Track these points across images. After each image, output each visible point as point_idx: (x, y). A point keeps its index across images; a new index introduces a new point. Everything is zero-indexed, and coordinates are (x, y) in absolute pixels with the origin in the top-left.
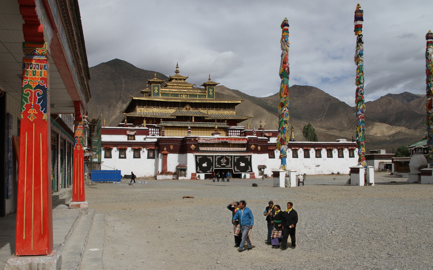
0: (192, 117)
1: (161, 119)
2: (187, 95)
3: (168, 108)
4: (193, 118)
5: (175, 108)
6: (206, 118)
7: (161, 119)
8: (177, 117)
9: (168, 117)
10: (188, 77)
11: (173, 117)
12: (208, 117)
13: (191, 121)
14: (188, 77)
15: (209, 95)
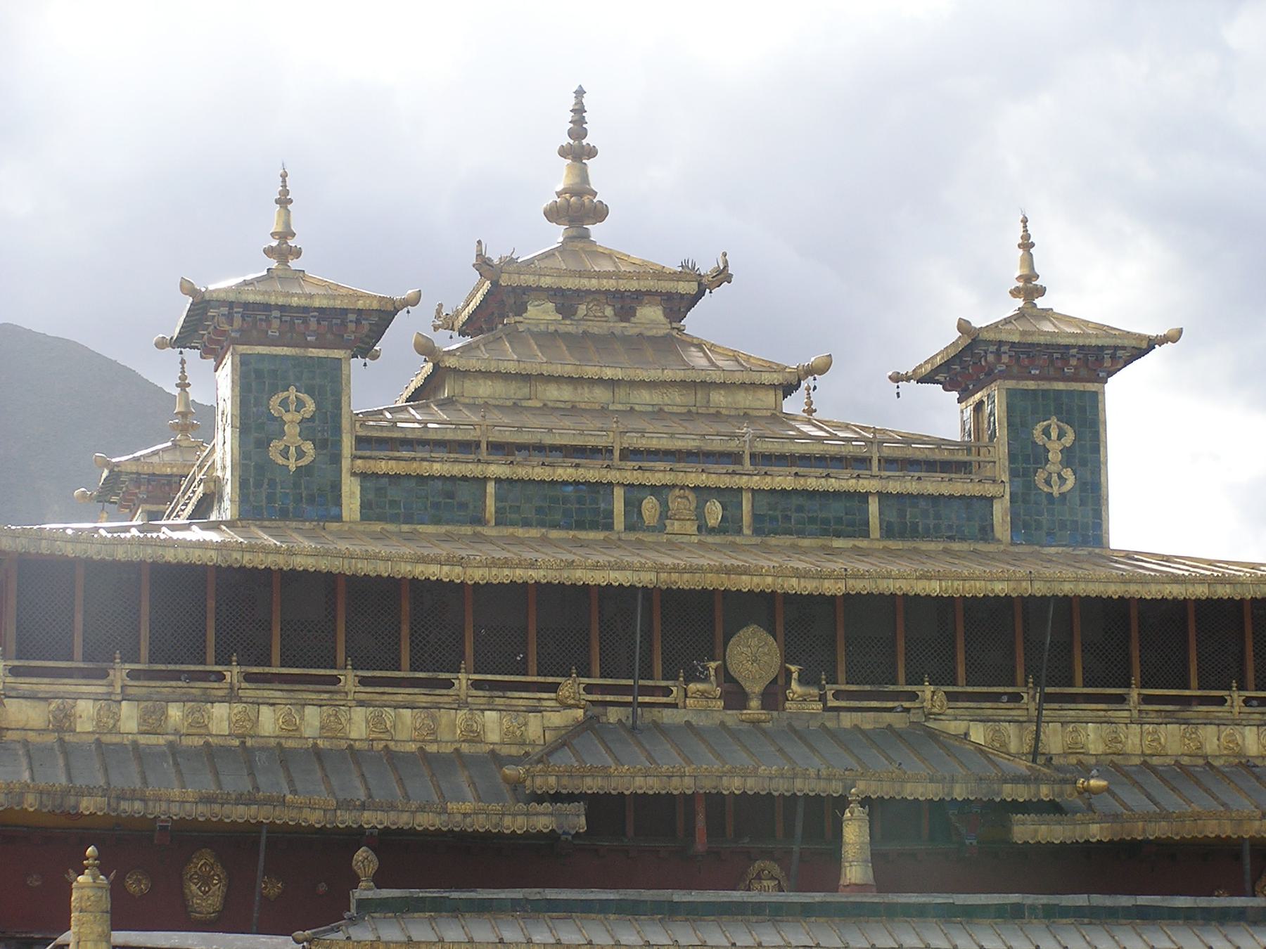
0: (823, 814)
1: (364, 860)
2: (729, 496)
3: (462, 680)
4: (854, 832)
5: (570, 687)
6: (1026, 830)
7: (364, 860)
8: (606, 810)
9: (466, 810)
10: (722, 276)
11: (543, 820)
12: (1053, 808)
13: (821, 865)
14: (722, 276)
15: (1024, 498)
